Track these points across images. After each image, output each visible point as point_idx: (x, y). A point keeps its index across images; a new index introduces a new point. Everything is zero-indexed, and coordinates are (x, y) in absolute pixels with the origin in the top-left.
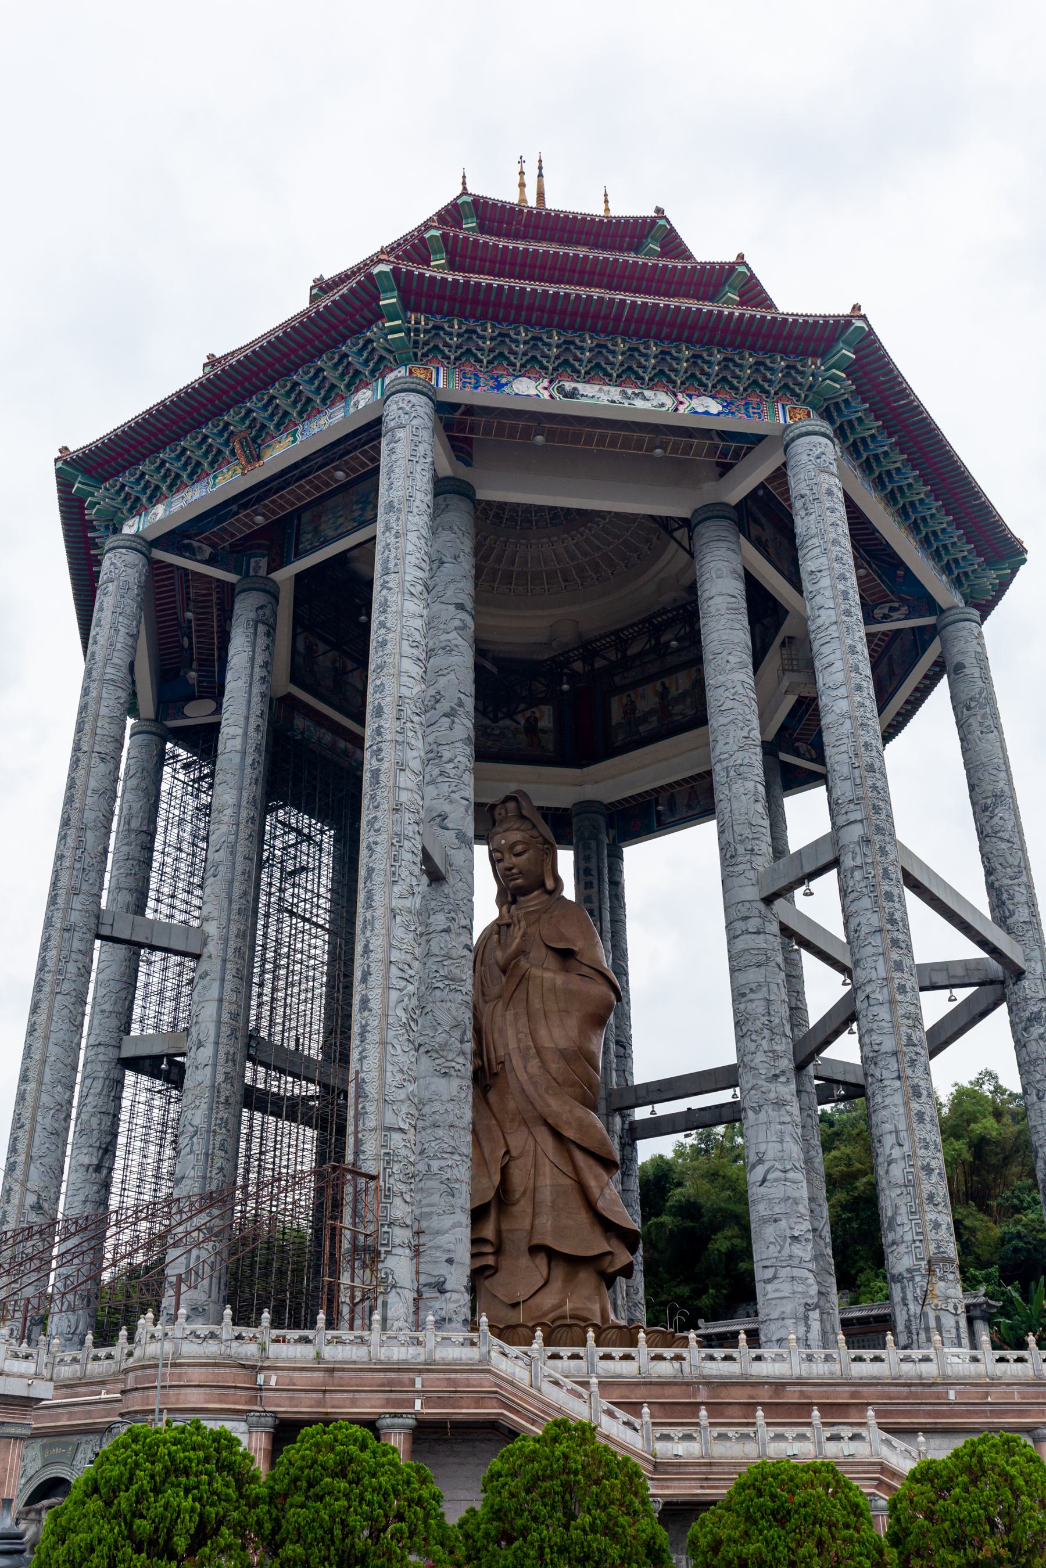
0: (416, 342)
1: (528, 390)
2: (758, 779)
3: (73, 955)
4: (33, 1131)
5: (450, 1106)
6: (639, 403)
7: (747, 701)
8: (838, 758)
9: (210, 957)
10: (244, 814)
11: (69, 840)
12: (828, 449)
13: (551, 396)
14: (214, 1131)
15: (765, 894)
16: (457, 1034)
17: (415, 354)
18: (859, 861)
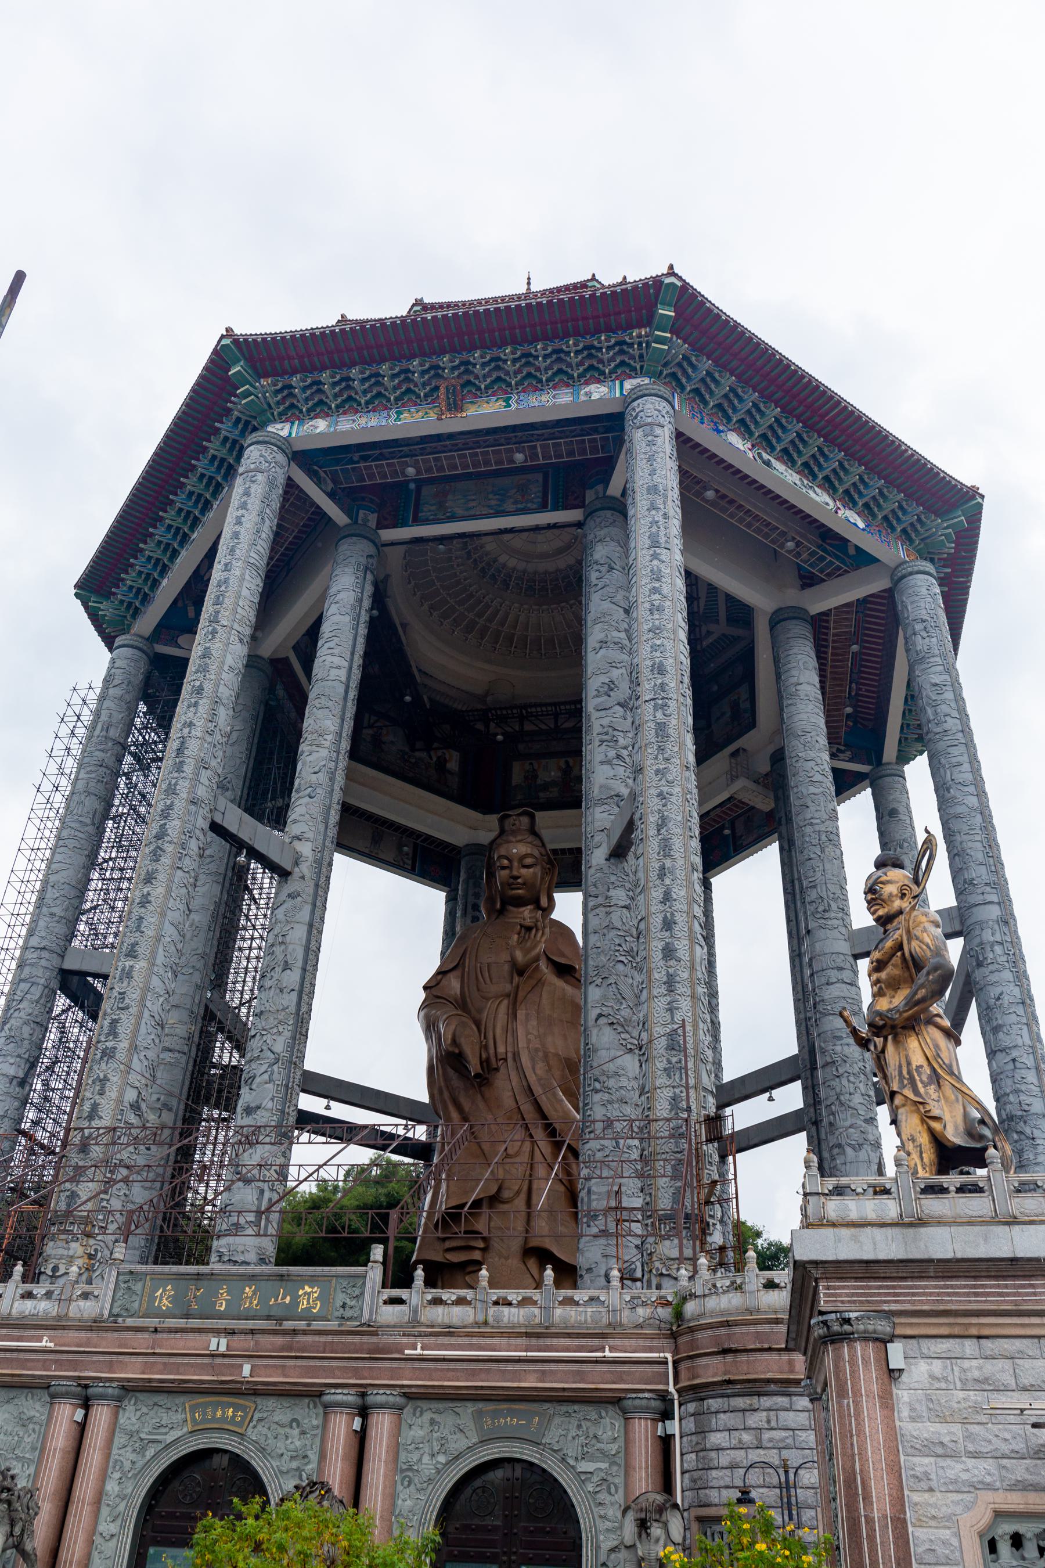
4: (140, 1016)
6: (812, 494)
8: (970, 844)
9: (303, 877)
11: (200, 708)
15: (857, 951)
17: (661, 372)
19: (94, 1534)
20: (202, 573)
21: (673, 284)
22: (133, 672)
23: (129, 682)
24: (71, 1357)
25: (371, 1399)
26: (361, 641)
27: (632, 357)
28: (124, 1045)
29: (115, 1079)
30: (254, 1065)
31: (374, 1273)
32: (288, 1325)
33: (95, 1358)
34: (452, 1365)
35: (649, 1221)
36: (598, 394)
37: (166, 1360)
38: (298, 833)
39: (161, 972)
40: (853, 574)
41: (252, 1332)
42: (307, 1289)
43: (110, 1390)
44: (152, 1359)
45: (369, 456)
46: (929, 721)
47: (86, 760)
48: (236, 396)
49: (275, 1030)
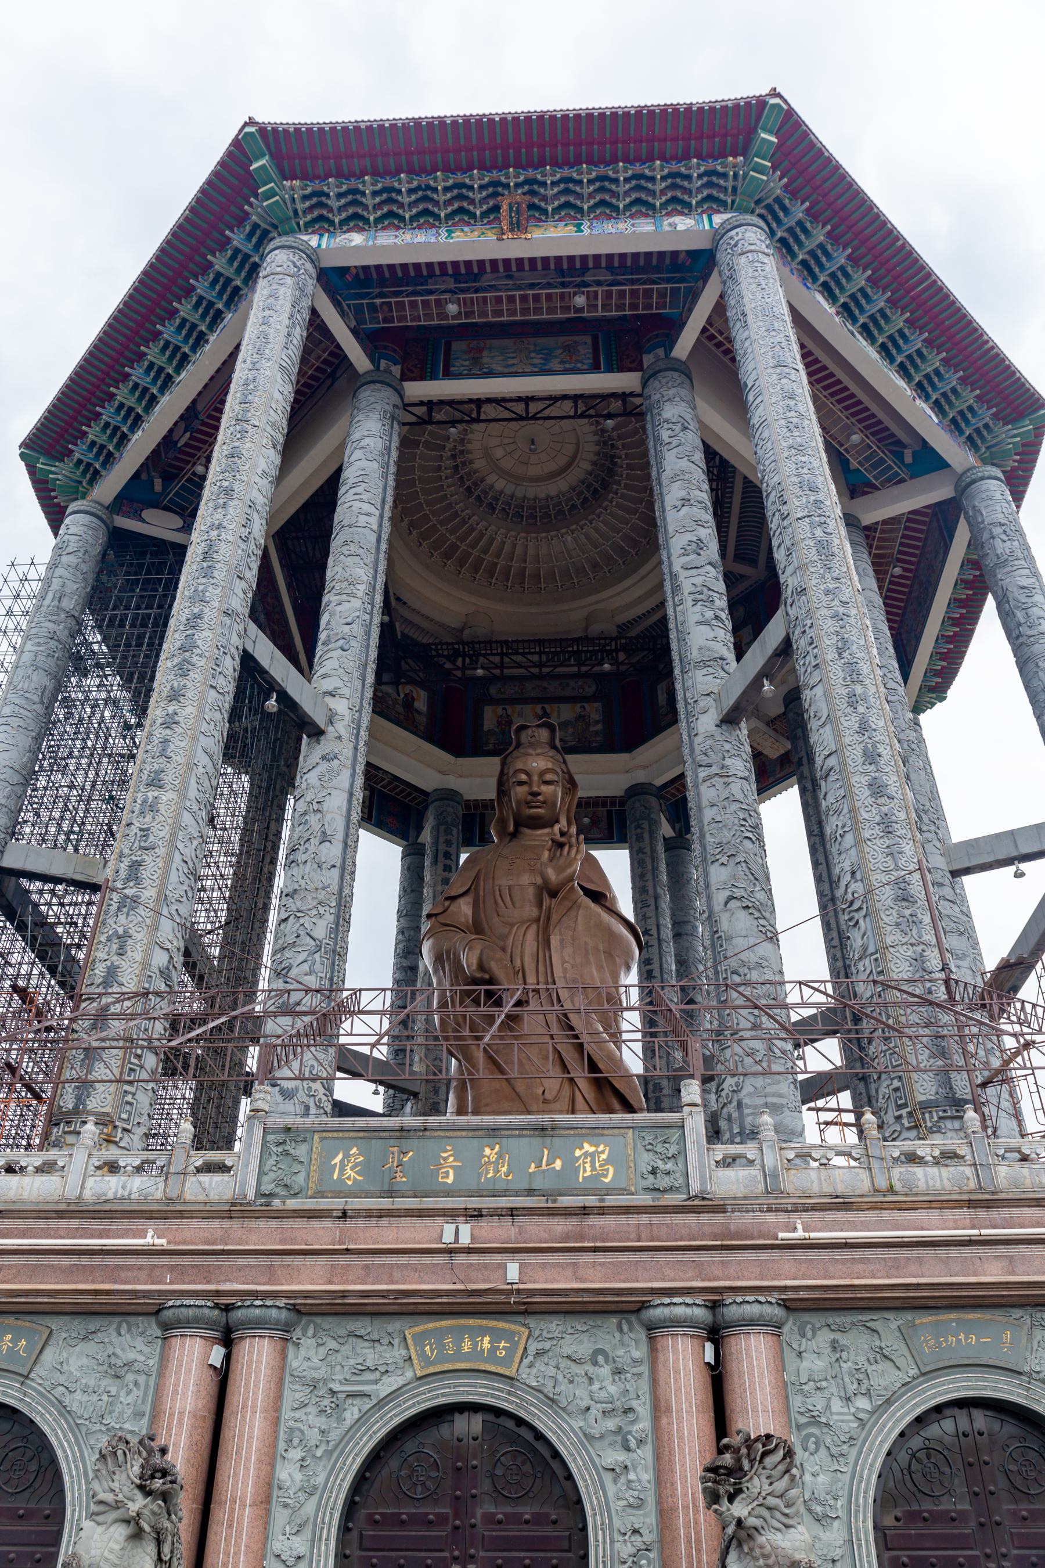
9: (339, 738)
11: (231, 510)
15: (955, 867)
19: (263, 1557)
20: (175, 438)
21: (778, 105)
22: (91, 540)
23: (86, 551)
24: (198, 1260)
25: (732, 1312)
26: (390, 492)
27: (725, 190)
28: (149, 894)
29: (139, 936)
30: (287, 954)
31: (696, 1124)
32: (565, 1201)
33: (241, 1261)
34: (858, 1254)
35: (904, 1112)
36: (683, 230)
37: (367, 1260)
38: (331, 688)
39: (195, 808)
40: (910, 483)
41: (513, 1213)
42: (587, 1147)
43: (274, 1313)
44: (342, 1260)
45: (402, 292)
46: (1020, 625)
47: (33, 631)
48: (256, 196)
49: (314, 912)
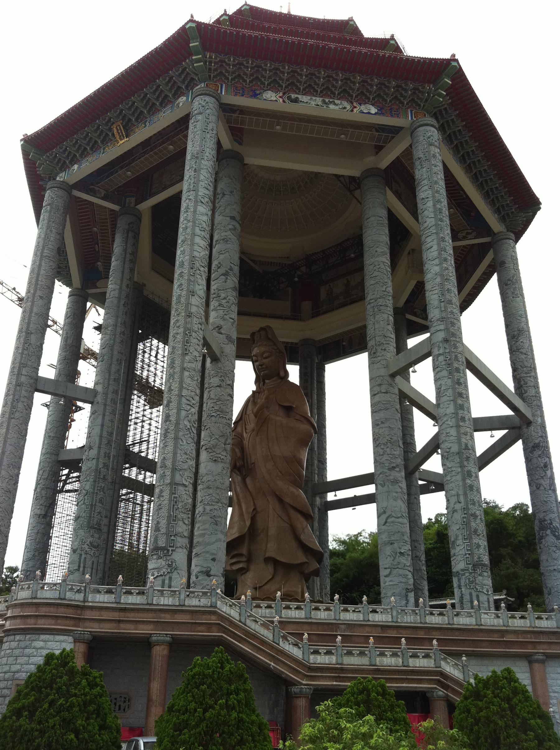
0: (210, 69)
1: (271, 99)
2: (390, 313)
3: (22, 399)
5: (217, 478)
6: (332, 107)
7: (385, 272)
8: (433, 297)
9: (98, 403)
10: (119, 330)
12: (434, 134)
13: (284, 101)
14: (97, 493)
15: (391, 372)
16: (223, 440)
17: (210, 76)
18: (441, 351)
